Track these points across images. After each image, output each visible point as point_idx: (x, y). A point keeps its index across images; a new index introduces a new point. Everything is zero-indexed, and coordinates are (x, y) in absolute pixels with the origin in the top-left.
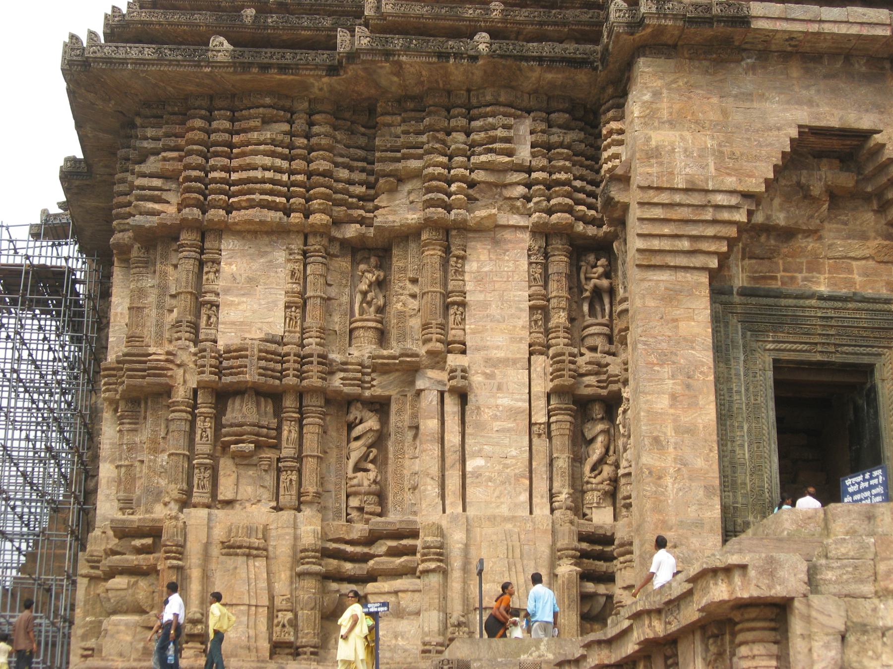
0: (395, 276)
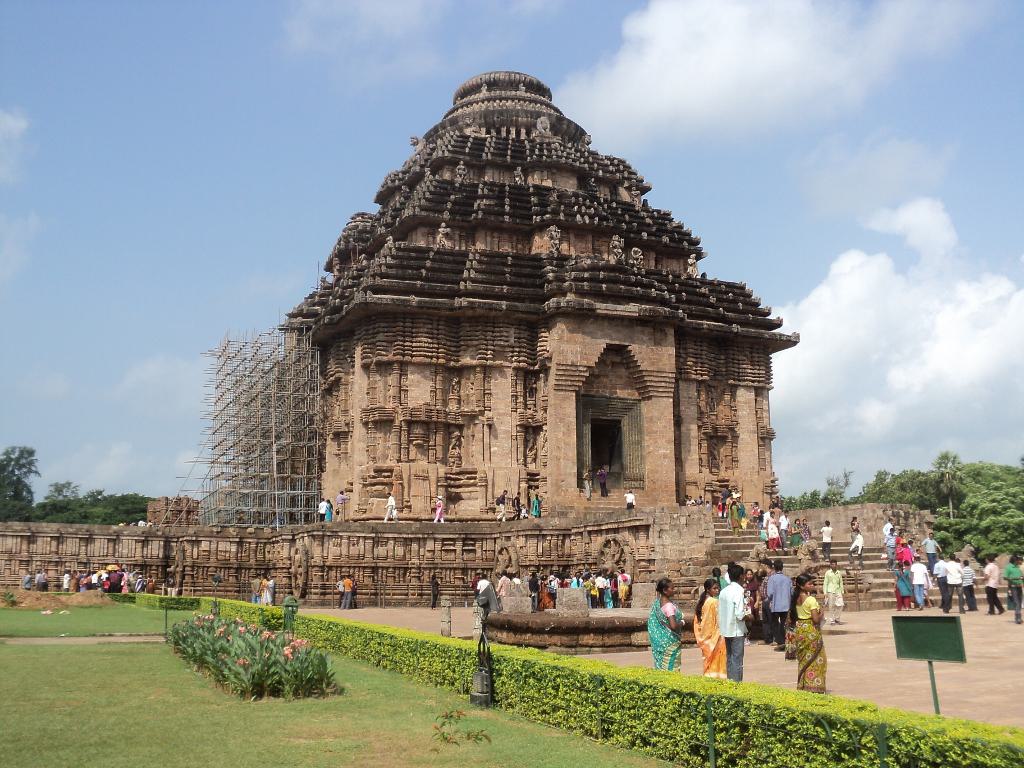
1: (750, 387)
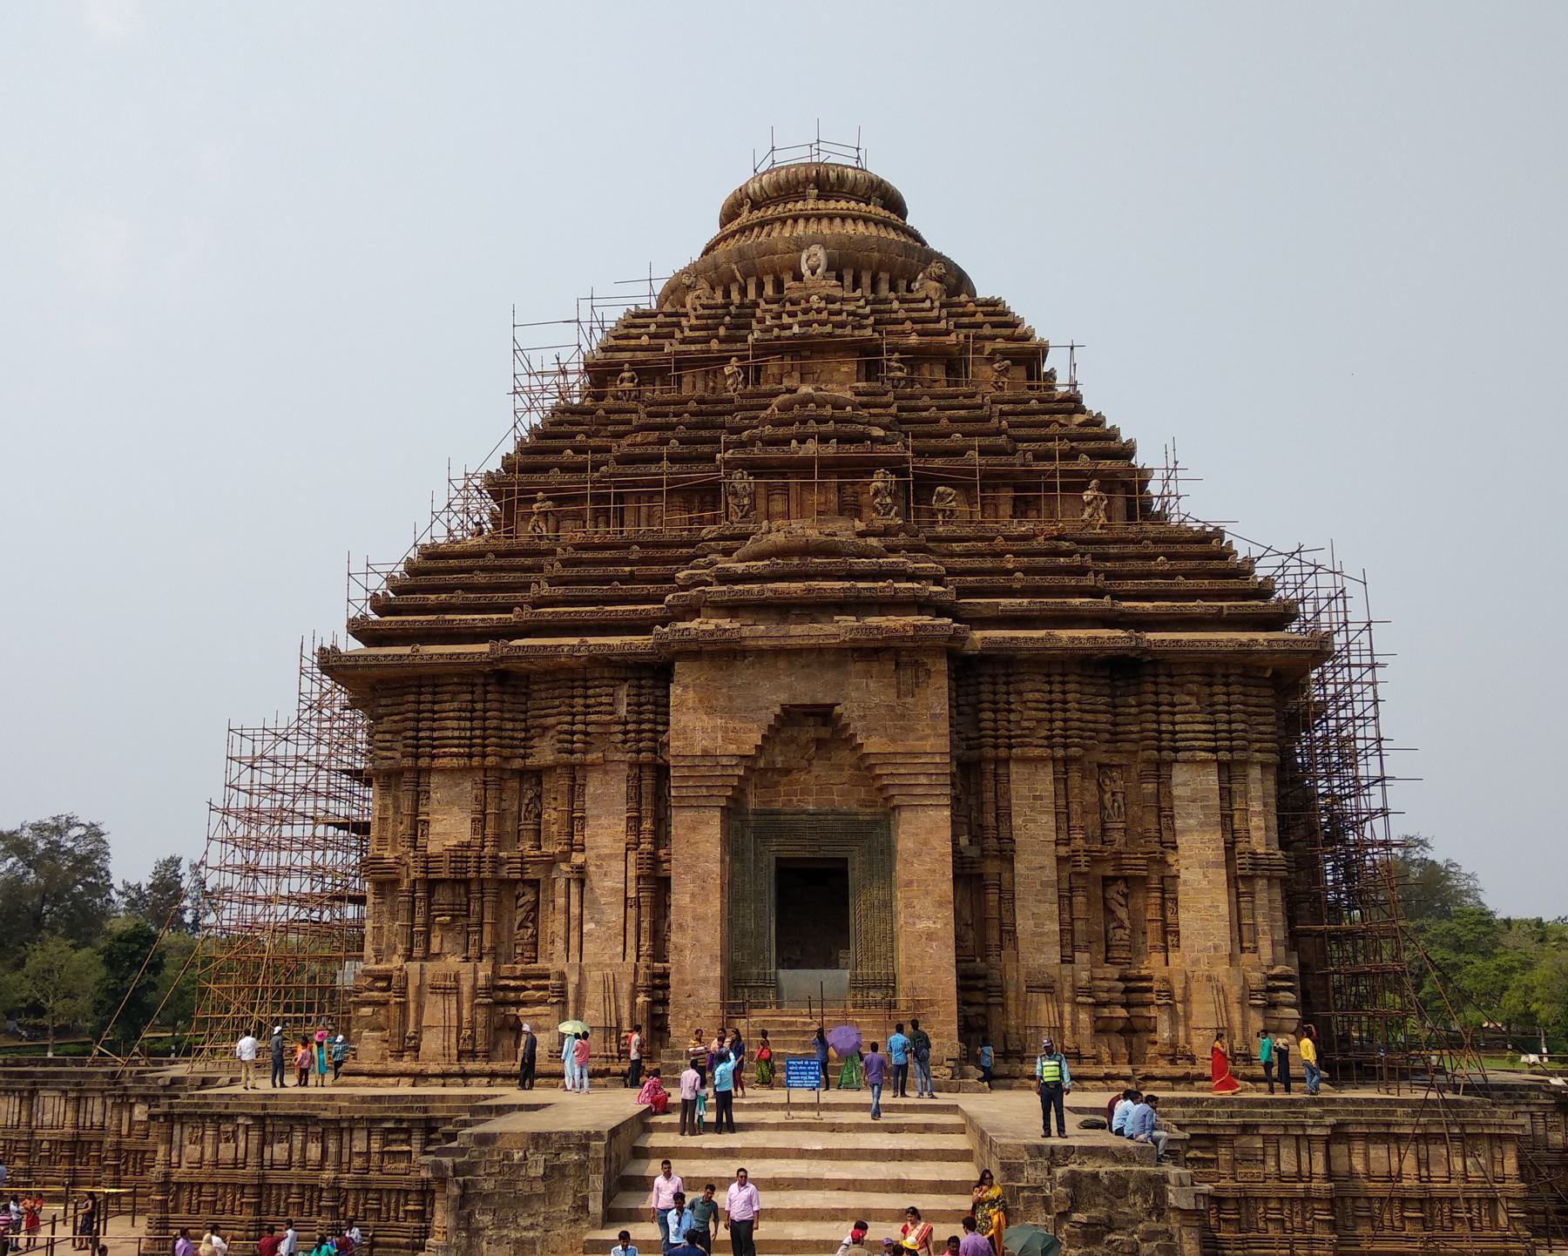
0: (544, 795)
1: (1204, 762)
